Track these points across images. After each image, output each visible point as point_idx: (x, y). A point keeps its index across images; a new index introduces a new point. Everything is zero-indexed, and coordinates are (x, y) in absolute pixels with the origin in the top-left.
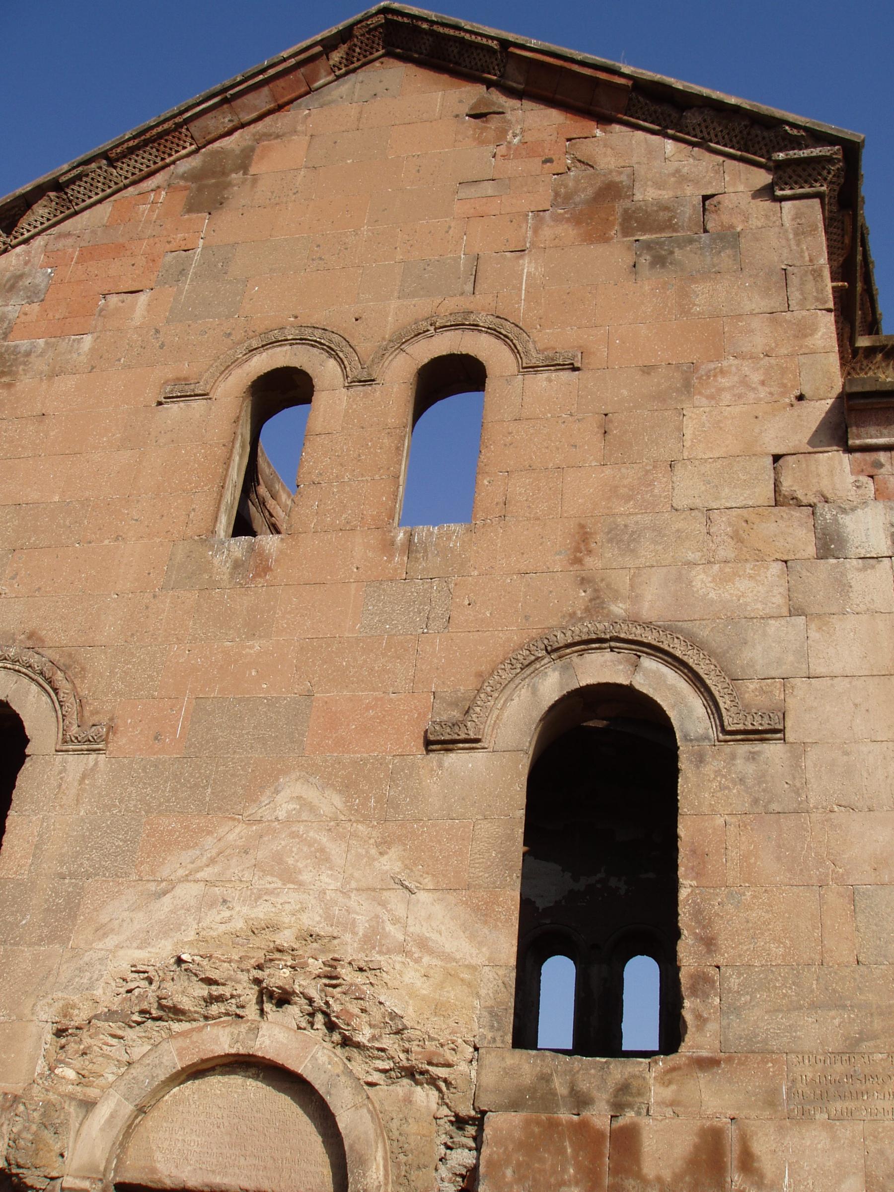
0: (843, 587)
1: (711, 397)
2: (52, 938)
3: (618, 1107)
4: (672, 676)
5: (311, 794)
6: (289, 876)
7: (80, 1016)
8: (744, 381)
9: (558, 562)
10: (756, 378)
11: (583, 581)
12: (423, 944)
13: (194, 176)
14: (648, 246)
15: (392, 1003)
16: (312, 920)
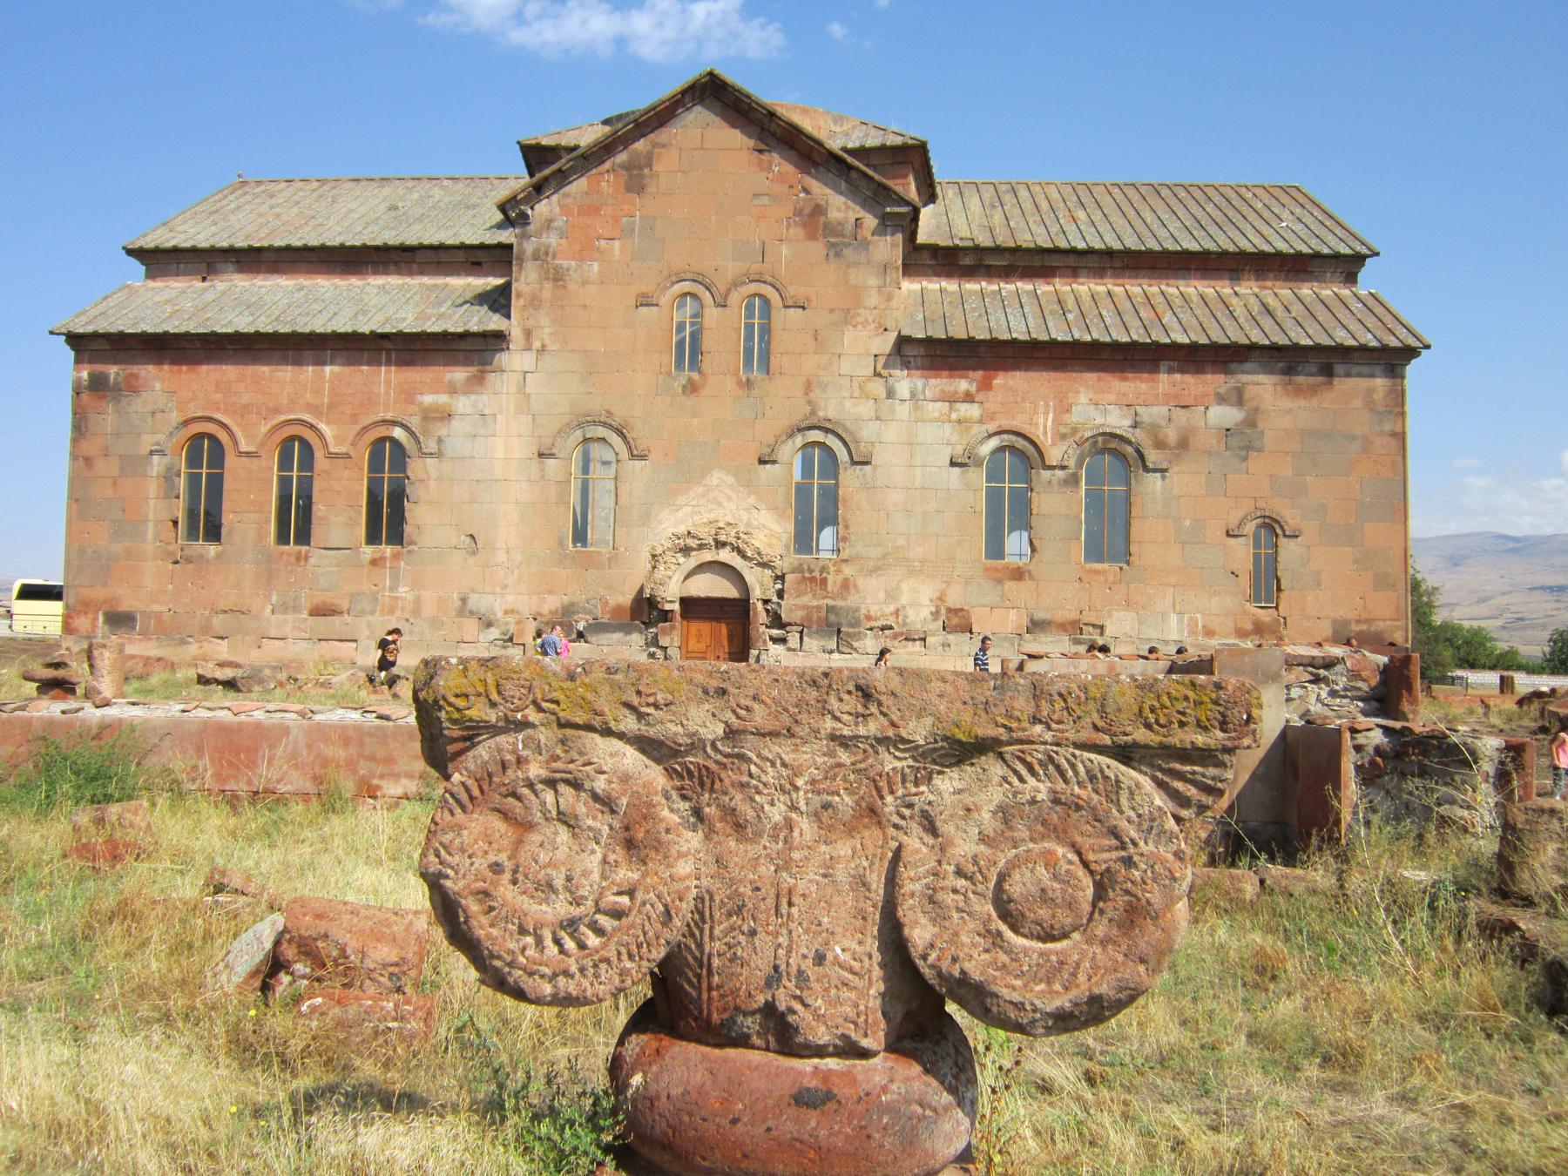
0: (893, 410)
1: (855, 326)
2: (643, 525)
3: (821, 573)
4: (837, 441)
5: (724, 477)
6: (720, 504)
7: (659, 551)
8: (866, 321)
9: (800, 393)
10: (870, 319)
11: (809, 402)
12: (764, 526)
13: (627, 167)
14: (833, 245)
15: (757, 545)
16: (729, 519)
